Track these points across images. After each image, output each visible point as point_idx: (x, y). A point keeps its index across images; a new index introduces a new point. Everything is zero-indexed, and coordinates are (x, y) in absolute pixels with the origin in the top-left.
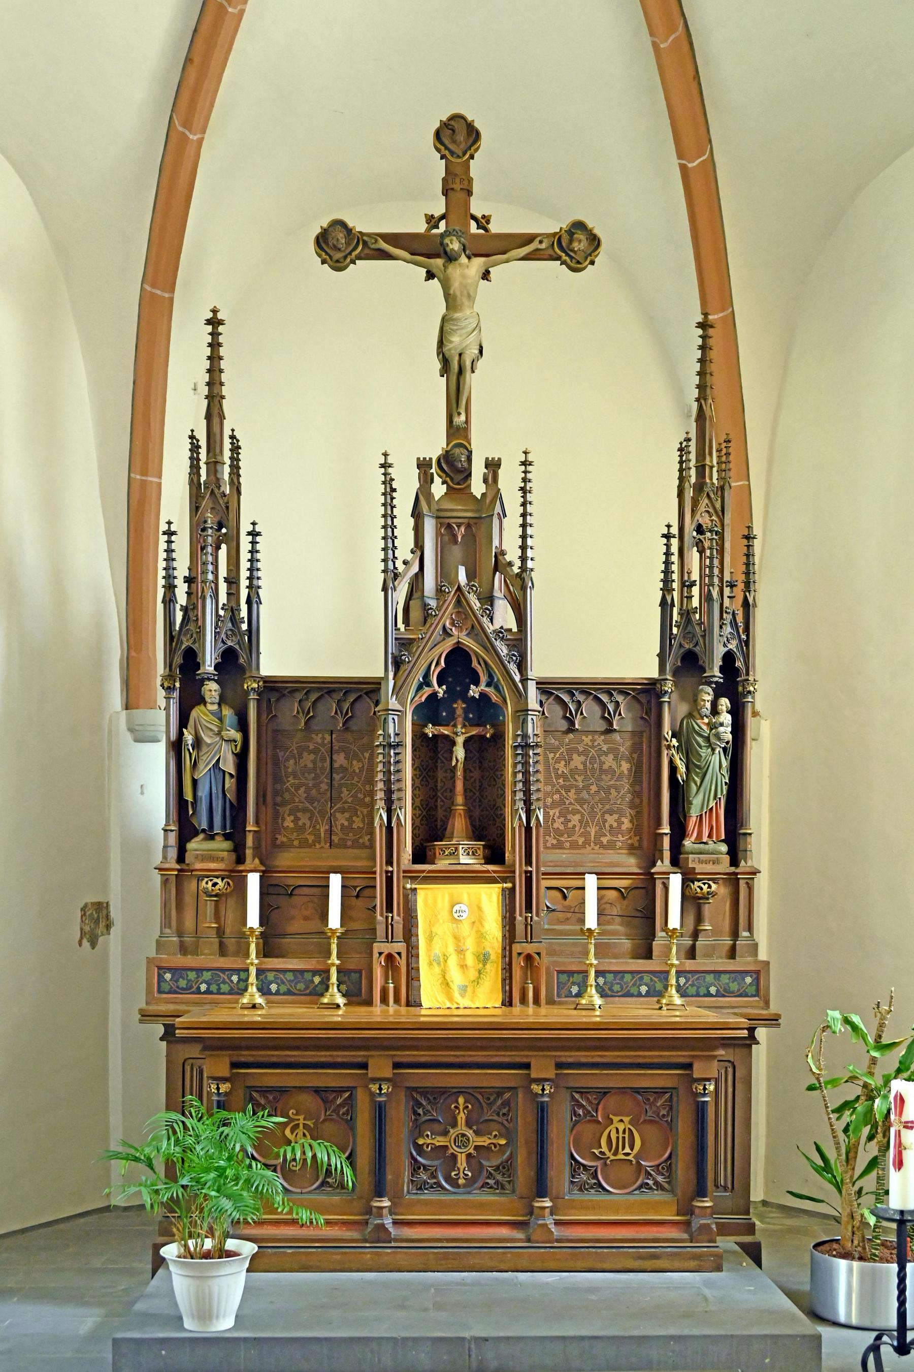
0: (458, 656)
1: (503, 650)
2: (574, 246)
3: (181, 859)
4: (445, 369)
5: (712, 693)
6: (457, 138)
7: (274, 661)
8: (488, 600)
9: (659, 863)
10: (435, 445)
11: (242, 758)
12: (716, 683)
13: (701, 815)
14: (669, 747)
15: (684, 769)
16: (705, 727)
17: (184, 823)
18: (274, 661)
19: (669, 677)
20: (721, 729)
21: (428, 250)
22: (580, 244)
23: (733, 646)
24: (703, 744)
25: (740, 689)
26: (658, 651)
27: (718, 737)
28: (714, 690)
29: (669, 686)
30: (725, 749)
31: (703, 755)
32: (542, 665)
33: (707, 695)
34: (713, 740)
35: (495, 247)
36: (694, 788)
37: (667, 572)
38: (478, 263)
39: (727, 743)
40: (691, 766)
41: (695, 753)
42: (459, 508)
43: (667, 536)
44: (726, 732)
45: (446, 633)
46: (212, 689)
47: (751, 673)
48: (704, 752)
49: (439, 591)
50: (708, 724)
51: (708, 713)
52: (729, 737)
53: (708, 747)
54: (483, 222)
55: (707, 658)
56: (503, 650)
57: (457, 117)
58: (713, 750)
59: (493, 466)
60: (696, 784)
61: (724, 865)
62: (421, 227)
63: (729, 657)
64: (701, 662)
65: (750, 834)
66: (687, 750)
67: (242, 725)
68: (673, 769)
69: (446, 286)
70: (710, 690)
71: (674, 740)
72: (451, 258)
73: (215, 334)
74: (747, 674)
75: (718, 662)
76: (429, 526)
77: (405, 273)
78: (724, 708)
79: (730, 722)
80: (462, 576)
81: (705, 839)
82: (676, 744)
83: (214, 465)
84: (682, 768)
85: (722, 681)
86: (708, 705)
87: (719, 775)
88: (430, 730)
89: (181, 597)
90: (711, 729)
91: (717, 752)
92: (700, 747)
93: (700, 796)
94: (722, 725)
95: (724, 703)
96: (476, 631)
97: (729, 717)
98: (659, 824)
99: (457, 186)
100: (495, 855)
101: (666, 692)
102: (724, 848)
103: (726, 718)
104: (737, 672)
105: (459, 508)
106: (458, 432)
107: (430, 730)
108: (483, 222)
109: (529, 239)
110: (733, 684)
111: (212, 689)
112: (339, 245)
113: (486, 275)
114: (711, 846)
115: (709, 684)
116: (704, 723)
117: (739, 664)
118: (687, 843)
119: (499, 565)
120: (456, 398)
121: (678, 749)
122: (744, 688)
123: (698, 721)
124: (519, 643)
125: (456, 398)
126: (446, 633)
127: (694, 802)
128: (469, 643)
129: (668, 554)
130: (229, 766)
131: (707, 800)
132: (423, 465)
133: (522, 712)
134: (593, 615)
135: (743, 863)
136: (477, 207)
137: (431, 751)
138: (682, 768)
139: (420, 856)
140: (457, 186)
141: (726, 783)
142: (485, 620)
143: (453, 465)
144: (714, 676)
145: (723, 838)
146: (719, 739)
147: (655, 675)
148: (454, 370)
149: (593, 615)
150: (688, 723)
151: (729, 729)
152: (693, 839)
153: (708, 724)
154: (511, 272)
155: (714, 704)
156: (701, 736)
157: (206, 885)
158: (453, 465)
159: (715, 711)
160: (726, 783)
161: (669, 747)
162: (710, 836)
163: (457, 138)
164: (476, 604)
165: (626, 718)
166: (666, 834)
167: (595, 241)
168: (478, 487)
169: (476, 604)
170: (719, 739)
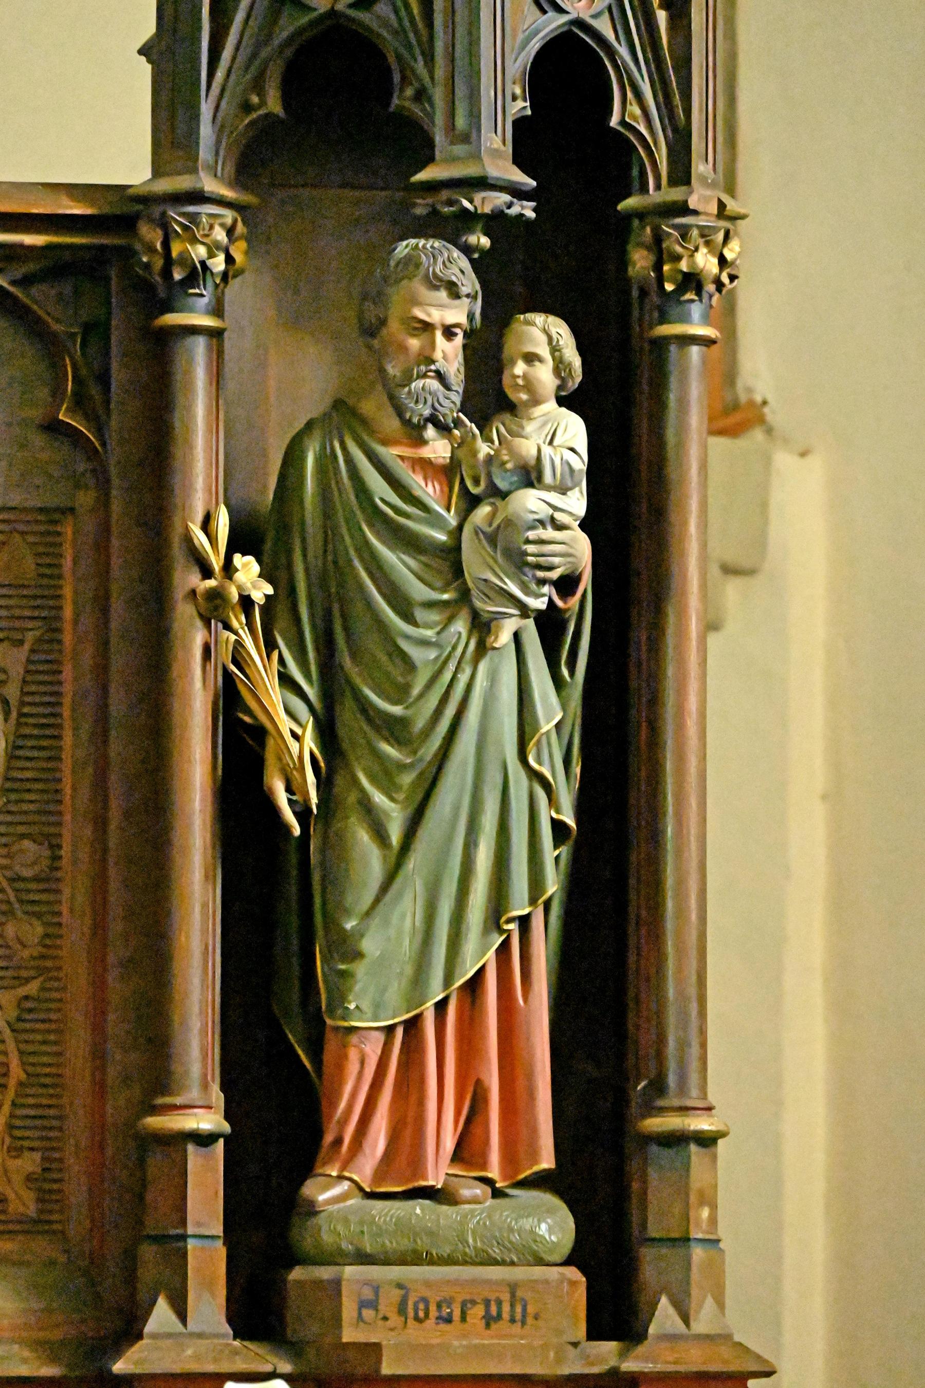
5: (469, 283)
9: (161, 1315)
12: (495, 222)
13: (413, 1025)
14: (213, 608)
15: (310, 743)
16: (429, 491)
19: (210, 186)
20: (531, 502)
24: (419, 591)
25: (640, 261)
26: (148, 28)
27: (509, 547)
28: (482, 264)
29: (211, 239)
30: (550, 625)
31: (420, 655)
33: (444, 305)
34: (477, 563)
36: (368, 858)
39: (567, 585)
40: (348, 718)
41: (372, 643)
44: (557, 516)
47: (700, 168)
48: (429, 639)
50: (448, 472)
51: (451, 404)
52: (580, 548)
53: (449, 610)
58: (482, 627)
60: (380, 835)
63: (568, 72)
64: (402, 99)
65: (707, 1141)
66: (329, 627)
68: (243, 744)
70: (461, 271)
71: (247, 568)
74: (681, 174)
75: (503, 97)
78: (545, 376)
79: (580, 464)
81: (435, 1176)
82: (261, 591)
84: (295, 736)
85: (528, 210)
86: (449, 354)
87: (520, 783)
90: (472, 502)
91: (504, 637)
92: (404, 607)
93: (407, 911)
94: (531, 476)
95: (545, 344)
97: (574, 430)
98: (157, 1080)
101: (197, 274)
102: (551, 1224)
103: (559, 437)
104: (616, 160)
114: (475, 1214)
115: (452, 227)
116: (424, 465)
117: (632, 111)
118: (327, 1193)
121: (271, 618)
122: (660, 255)
123: (390, 453)
127: (370, 945)
135: (664, 1317)
138: (295, 736)
141: (558, 827)
144: (482, 183)
145: (547, 1162)
146: (518, 562)
147: (128, 162)
150: (326, 463)
151: (576, 503)
152: (364, 1170)
153: (448, 472)
155: (486, 354)
156: (409, 542)
159: (490, 396)
160: (558, 827)
161: (213, 608)
162: (466, 1152)
166: (204, 1140)
170: (518, 562)
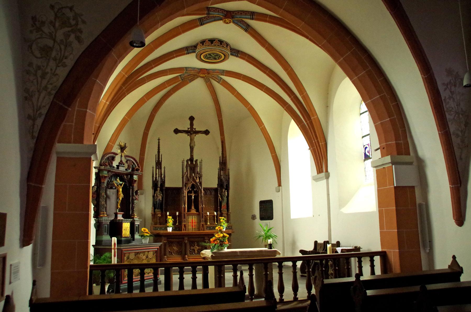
0: (193, 185)
2: (207, 132)
3: (154, 211)
4: (191, 147)
6: (192, 119)
7: (167, 185)
8: (197, 178)
10: (189, 157)
11: (162, 198)
17: (155, 206)
18: (167, 185)
32: (204, 185)
33: (224, 190)
42: (192, 166)
46: (159, 189)
54: (195, 129)
55: (223, 184)
57: (192, 116)
59: (196, 160)
61: (226, 212)
62: (187, 129)
63: (227, 185)
67: (163, 194)
69: (190, 137)
72: (191, 134)
76: (189, 168)
77: (184, 135)
88: (189, 194)
99: (192, 124)
100: (197, 210)
105: (192, 166)
107: (189, 194)
108: (195, 129)
109: (201, 131)
110: (227, 189)
111: (159, 189)
112: (177, 131)
124: (201, 183)
130: (161, 199)
131: (224, 204)
133: (201, 192)
134: (210, 180)
136: (194, 127)
137: (189, 197)
139: (188, 211)
140: (192, 124)
143: (191, 159)
148: (192, 149)
149: (210, 180)
157: (158, 215)
158: (191, 159)
163: (192, 119)
165: (213, 193)
167: (209, 132)
168: (194, 163)
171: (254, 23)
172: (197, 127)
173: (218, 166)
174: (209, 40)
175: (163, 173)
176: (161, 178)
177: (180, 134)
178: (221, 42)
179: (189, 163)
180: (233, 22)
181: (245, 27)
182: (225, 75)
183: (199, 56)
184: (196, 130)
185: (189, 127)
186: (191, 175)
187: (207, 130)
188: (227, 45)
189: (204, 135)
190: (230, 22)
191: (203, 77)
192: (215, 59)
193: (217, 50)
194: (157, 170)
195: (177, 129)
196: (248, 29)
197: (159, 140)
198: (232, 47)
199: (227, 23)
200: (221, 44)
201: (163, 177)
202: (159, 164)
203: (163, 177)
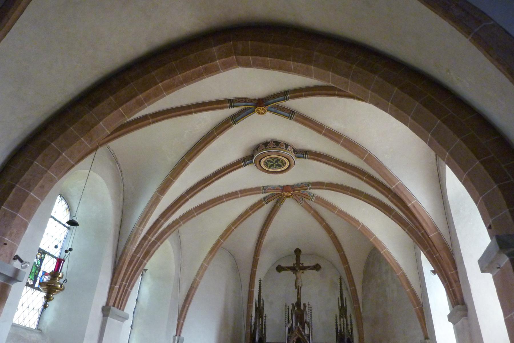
1: (306, 338)
2: (317, 267)
8: (303, 328)
10: (294, 301)
21: (293, 269)
22: (318, 267)
23: (349, 337)
35: (304, 268)
37: (336, 323)
38: (301, 271)
42: (299, 313)
43: (336, 316)
45: (296, 335)
49: (295, 328)
56: (306, 338)
57: (297, 249)
62: (292, 265)
73: (260, 283)
77: (290, 273)
80: (299, 324)
83: (259, 305)
89: (253, 328)
96: (301, 334)
99: (298, 259)
105: (299, 313)
106: (299, 299)
108: (303, 264)
112: (280, 269)
113: (303, 273)
119: (306, 322)
120: (299, 293)
125: (299, 293)
126: (296, 335)
128: (301, 337)
129: (336, 319)
132: (293, 304)
140: (298, 259)
142: (303, 333)
143: (298, 304)
148: (298, 289)
154: (308, 272)
158: (298, 304)
164: (301, 329)
169: (301, 329)
171: (293, 104)
172: (305, 262)
173: (337, 311)
174: (263, 144)
175: (349, 323)
176: (348, 331)
177: (283, 272)
178: (277, 143)
179: (296, 308)
180: (268, 110)
181: (288, 115)
182: (312, 189)
183: (258, 165)
184: (304, 265)
185: (295, 262)
186: (296, 324)
187: (317, 265)
188: (287, 146)
189: (314, 271)
190: (265, 112)
191: (290, 196)
192: (280, 166)
193: (272, 153)
194: (342, 319)
195: (279, 265)
196: (291, 114)
197: (260, 281)
198: (297, 148)
199: (262, 114)
200: (277, 145)
201: (349, 328)
202: (260, 311)
203: (349, 328)
